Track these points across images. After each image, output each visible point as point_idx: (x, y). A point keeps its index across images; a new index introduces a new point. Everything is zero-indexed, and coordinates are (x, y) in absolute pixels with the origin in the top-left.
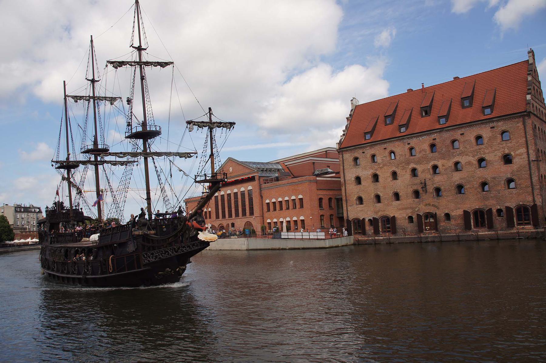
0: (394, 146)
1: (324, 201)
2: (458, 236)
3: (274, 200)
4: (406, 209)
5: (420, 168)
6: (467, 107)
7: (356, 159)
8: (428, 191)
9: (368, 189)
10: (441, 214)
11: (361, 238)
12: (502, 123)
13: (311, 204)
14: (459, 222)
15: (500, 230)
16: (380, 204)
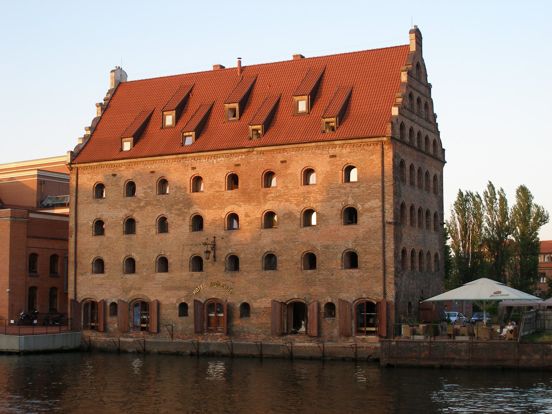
1: (39, 260)
4: (178, 288)
5: (209, 216)
12: (348, 150)
14: (264, 320)
15: (329, 341)
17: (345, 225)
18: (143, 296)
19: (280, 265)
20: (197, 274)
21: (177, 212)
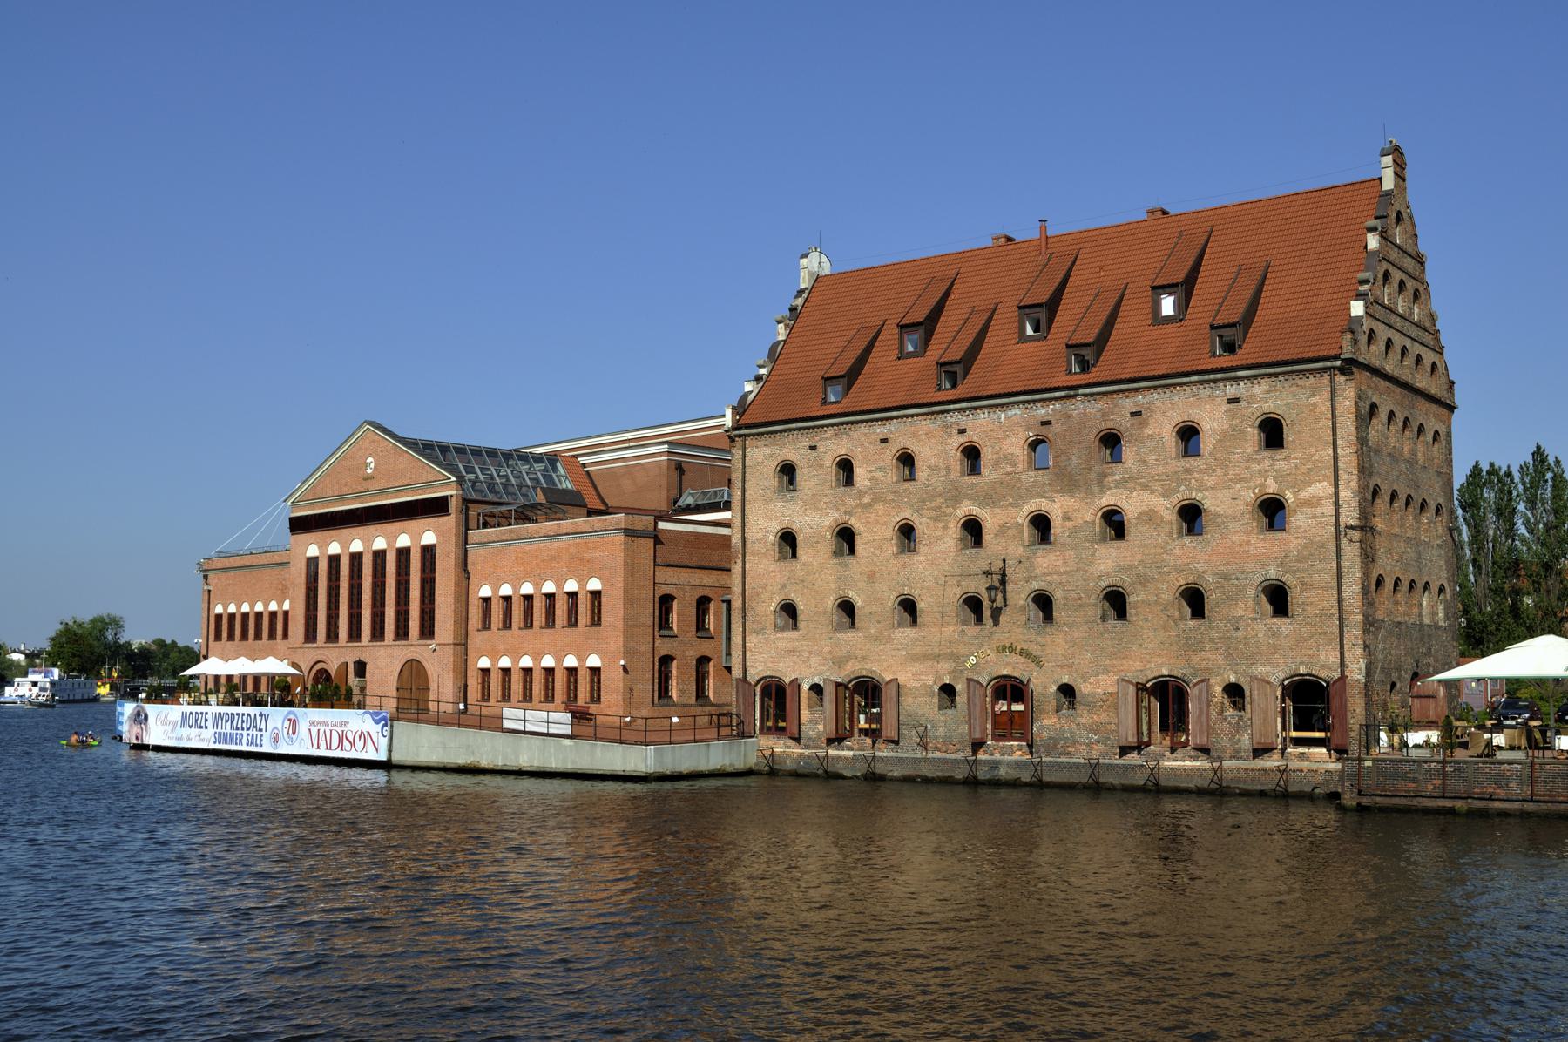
0: (914, 435)
2: (1095, 767)
3: (506, 590)
4: (936, 657)
5: (991, 522)
6: (1031, 339)
7: (788, 471)
10: (1043, 684)
11: (782, 747)
16: (851, 634)
17: (1261, 532)
20: (973, 630)
21: (934, 514)
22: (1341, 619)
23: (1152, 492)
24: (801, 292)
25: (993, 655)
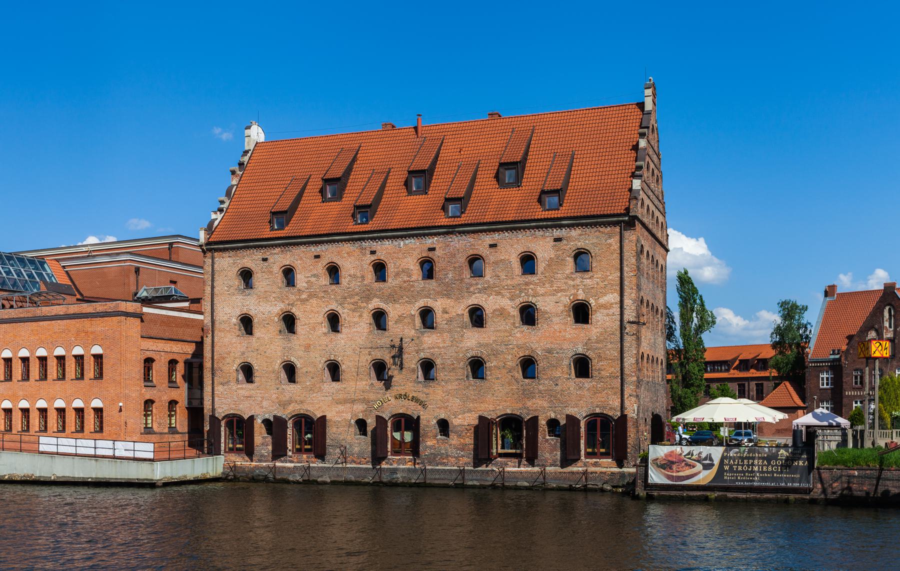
2: (462, 472)
4: (353, 401)
5: (393, 312)
7: (246, 275)
8: (406, 365)
9: (268, 348)
10: (428, 420)
11: (241, 461)
13: (125, 371)
15: (551, 465)
16: (292, 386)
18: (307, 411)
19: (488, 373)
22: (622, 379)
23: (503, 296)
24: (246, 152)
25: (393, 400)
